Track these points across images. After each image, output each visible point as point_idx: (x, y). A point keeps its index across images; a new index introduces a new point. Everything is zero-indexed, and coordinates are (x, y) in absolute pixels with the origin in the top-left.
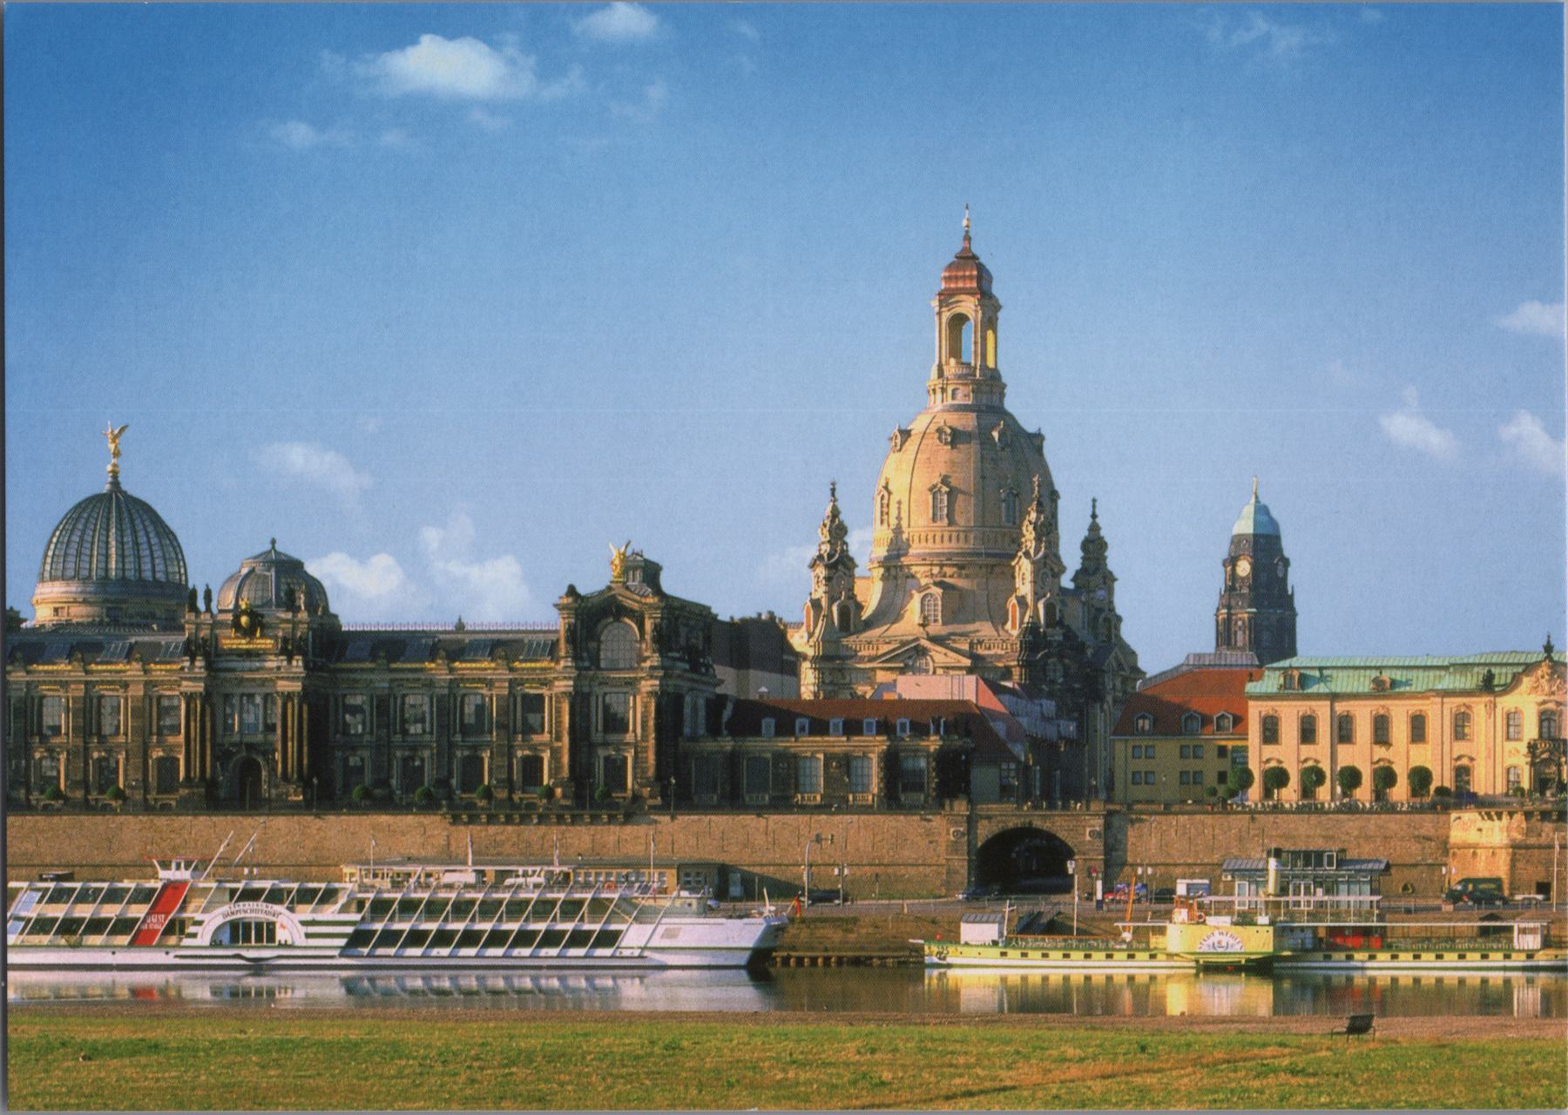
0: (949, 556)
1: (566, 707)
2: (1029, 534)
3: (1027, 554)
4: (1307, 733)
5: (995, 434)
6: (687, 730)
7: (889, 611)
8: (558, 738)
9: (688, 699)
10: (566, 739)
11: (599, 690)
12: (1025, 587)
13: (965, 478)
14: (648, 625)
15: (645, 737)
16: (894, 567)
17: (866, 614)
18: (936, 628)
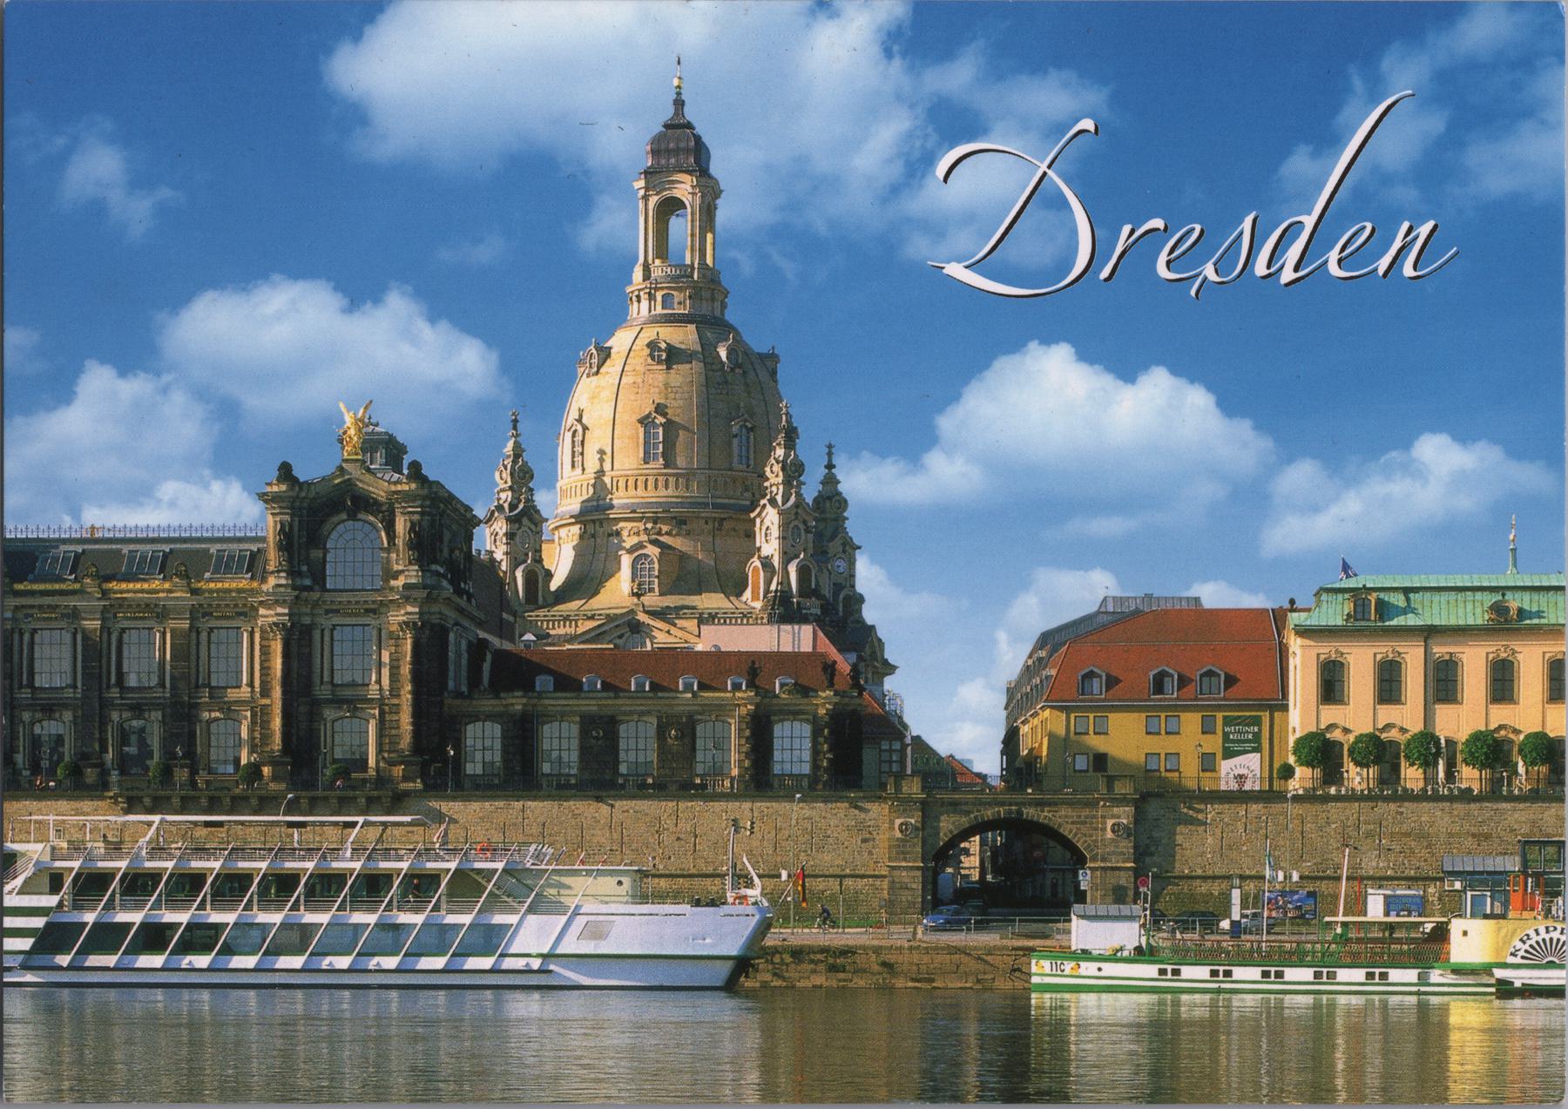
0: (666, 507)
1: (277, 647)
2: (774, 476)
3: (773, 502)
4: (1388, 686)
5: (723, 353)
6: (451, 684)
7: (585, 581)
8: (266, 692)
9: (452, 636)
10: (277, 692)
11: (325, 622)
12: (770, 547)
13: (684, 409)
14: (401, 525)
15: (395, 692)
16: (595, 517)
17: (555, 584)
18: (653, 600)
